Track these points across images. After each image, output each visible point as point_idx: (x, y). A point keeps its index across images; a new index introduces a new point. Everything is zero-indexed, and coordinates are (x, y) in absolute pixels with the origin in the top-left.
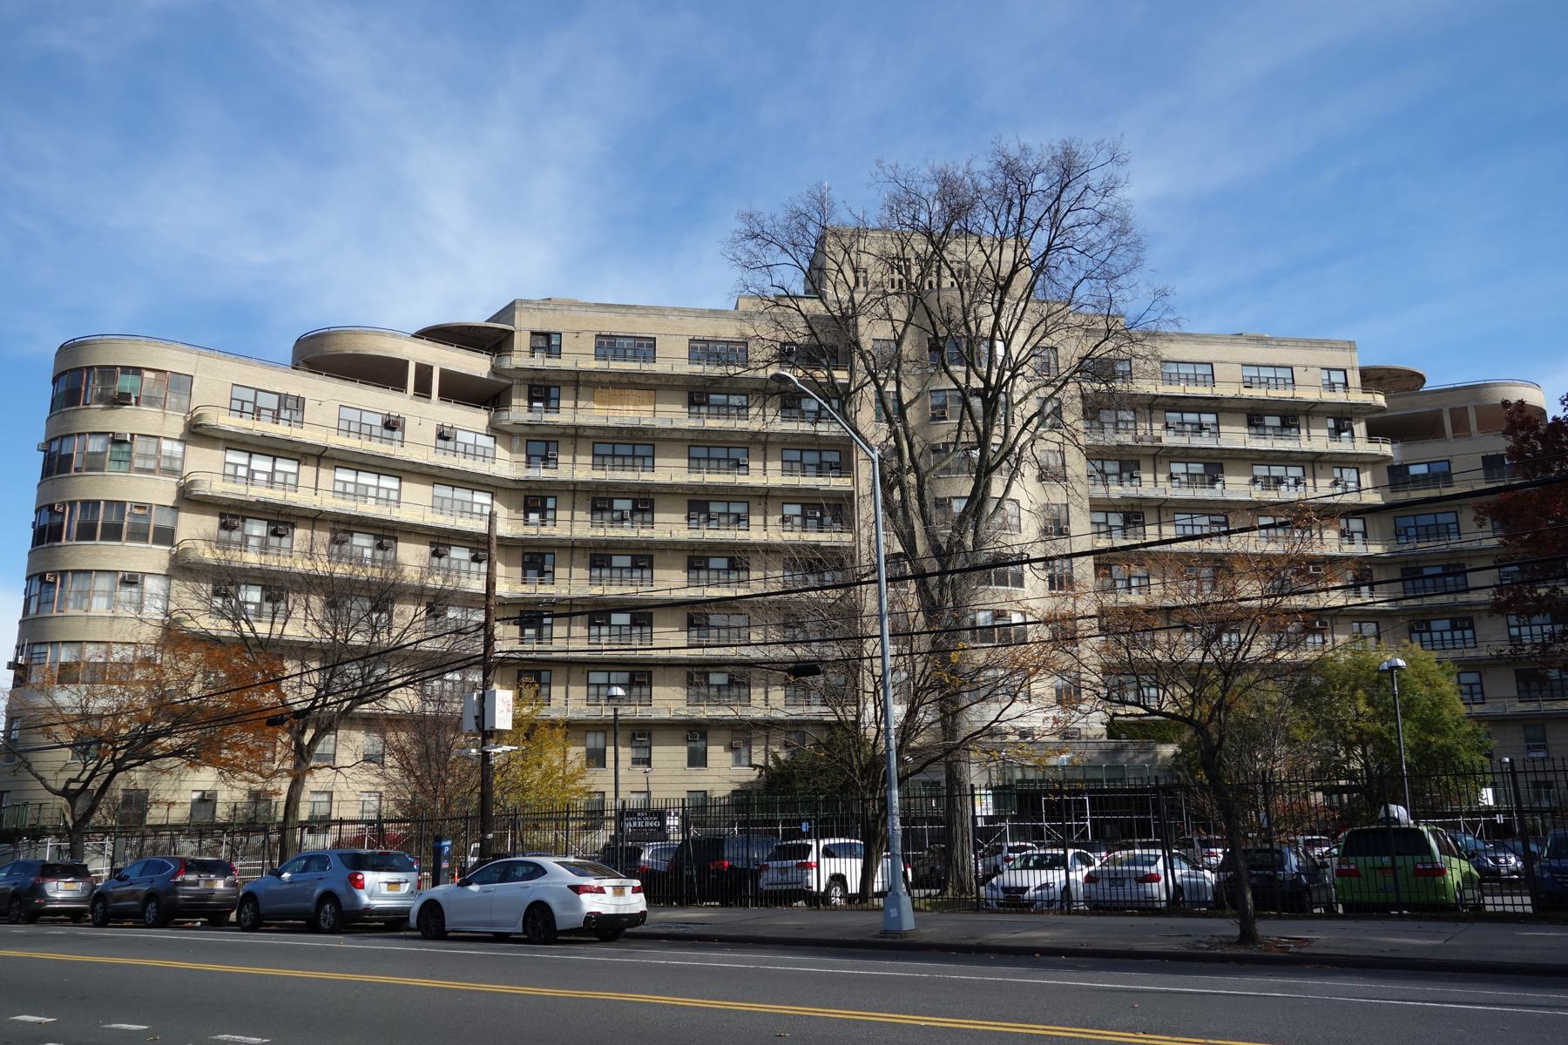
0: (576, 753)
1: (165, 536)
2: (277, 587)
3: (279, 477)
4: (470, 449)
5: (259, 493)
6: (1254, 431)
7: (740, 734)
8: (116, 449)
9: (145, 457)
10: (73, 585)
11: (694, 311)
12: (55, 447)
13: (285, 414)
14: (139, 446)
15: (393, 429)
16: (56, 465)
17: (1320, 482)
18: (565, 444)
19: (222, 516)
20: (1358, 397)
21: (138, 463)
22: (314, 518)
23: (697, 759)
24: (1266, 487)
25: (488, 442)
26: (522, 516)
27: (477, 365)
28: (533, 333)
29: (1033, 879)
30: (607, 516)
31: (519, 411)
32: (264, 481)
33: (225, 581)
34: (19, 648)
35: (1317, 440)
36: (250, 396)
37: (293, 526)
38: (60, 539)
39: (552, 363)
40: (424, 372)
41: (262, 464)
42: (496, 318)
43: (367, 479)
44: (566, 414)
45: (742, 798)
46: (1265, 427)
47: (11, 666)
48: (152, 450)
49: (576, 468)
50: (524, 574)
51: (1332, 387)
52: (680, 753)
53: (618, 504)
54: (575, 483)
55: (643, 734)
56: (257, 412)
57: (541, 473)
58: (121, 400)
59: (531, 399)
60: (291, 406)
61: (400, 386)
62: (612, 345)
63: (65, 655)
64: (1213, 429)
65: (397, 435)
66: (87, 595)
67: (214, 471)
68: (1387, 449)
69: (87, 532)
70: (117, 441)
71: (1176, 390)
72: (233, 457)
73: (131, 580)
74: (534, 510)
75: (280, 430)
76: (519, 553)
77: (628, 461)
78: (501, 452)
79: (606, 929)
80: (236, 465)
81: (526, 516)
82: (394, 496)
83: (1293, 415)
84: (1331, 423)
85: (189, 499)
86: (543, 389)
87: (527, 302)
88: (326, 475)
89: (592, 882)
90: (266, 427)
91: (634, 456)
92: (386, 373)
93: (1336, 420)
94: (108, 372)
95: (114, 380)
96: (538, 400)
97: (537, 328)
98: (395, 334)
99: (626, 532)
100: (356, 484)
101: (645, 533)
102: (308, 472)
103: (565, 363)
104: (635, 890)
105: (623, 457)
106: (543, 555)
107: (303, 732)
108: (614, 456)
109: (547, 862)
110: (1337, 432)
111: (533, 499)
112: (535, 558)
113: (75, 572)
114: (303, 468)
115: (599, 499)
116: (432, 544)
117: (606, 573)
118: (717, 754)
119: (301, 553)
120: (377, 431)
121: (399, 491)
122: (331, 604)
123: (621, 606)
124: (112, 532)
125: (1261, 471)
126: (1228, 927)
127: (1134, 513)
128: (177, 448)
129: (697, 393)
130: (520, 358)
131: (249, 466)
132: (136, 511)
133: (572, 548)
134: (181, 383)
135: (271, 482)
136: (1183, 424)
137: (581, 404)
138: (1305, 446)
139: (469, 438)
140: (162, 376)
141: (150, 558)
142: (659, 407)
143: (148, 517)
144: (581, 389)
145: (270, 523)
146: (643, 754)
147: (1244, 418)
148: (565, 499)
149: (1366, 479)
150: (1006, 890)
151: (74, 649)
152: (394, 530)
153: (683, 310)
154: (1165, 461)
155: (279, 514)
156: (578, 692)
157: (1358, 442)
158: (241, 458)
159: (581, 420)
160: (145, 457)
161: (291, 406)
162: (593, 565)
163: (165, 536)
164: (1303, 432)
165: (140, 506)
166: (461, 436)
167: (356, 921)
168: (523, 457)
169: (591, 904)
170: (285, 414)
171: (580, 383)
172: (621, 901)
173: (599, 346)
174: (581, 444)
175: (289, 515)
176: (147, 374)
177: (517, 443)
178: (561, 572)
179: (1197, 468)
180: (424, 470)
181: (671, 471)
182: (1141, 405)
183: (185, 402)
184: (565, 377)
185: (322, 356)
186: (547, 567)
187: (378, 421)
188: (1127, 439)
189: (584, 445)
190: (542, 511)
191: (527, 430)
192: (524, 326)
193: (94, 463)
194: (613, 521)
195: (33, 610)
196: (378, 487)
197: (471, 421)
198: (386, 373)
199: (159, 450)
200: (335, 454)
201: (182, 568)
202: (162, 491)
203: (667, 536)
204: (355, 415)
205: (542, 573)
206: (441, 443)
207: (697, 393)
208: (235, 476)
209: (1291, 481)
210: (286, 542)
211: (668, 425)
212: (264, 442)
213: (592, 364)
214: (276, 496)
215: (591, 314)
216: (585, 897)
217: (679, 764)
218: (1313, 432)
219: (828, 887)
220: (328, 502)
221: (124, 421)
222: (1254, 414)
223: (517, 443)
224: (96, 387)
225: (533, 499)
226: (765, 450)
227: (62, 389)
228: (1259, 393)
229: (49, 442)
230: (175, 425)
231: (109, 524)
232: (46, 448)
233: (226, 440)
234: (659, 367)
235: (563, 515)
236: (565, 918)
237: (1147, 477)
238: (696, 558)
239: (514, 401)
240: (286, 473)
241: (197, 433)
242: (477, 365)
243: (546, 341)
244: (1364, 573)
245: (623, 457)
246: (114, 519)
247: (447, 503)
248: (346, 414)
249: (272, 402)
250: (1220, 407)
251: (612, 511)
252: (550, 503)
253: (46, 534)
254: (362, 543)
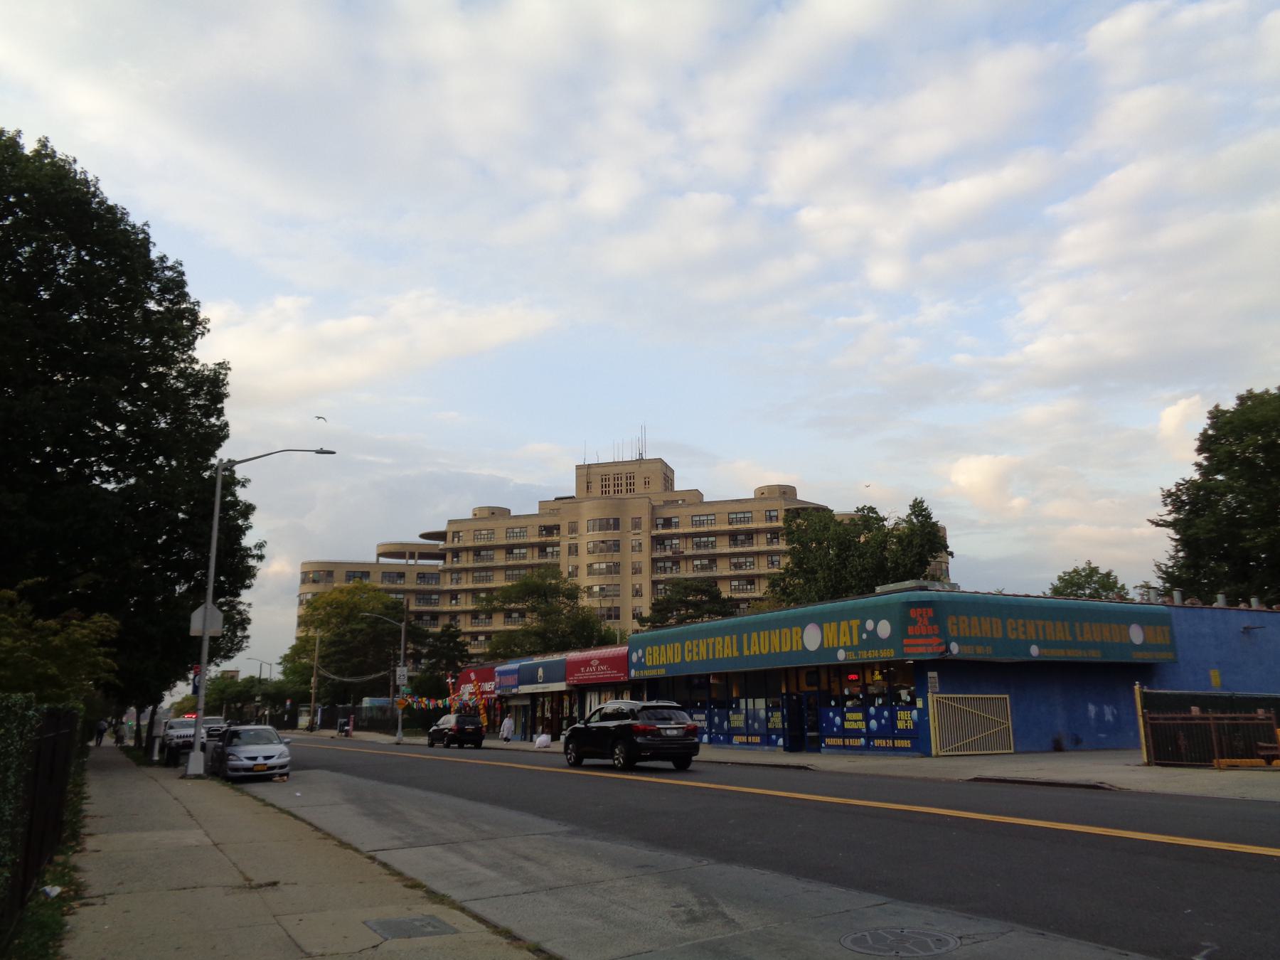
35: (761, 545)
51: (771, 519)
83: (750, 535)
103: (461, 544)
110: (770, 542)
125: (734, 560)
138: (755, 548)
157: (782, 546)
179: (706, 562)
188: (669, 553)
190: (456, 598)
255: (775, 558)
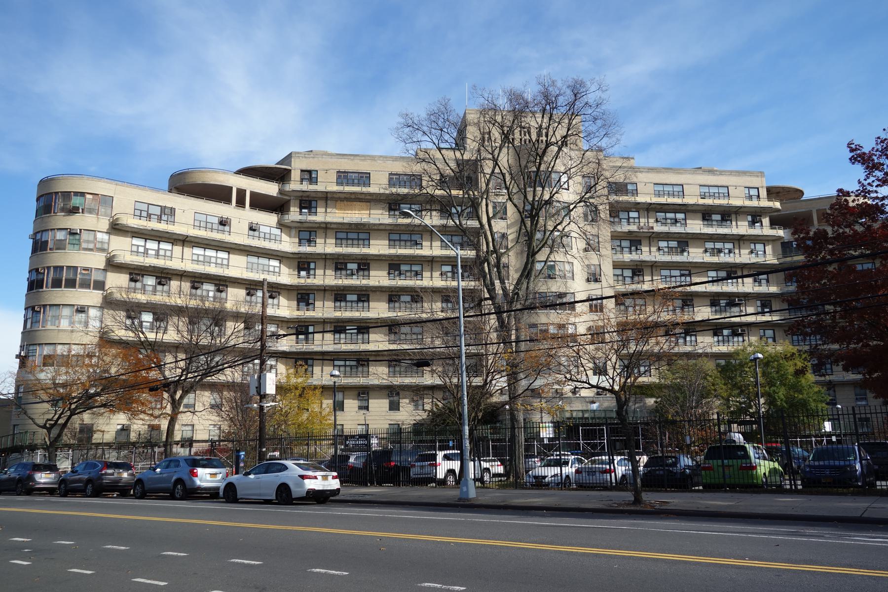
0: (328, 403)
1: (100, 285)
2: (162, 314)
3: (162, 253)
4: (267, 236)
5: (151, 261)
6: (706, 223)
7: (418, 392)
8: (71, 238)
9: (88, 242)
10: (50, 313)
11: (391, 157)
12: (39, 236)
13: (164, 218)
14: (85, 236)
15: (225, 225)
16: (39, 246)
17: (742, 251)
18: (320, 232)
19: (130, 274)
20: (765, 203)
21: (84, 245)
22: (181, 275)
23: (394, 407)
24: (712, 254)
25: (278, 232)
26: (296, 273)
27: (270, 189)
28: (302, 171)
29: (550, 472)
30: (344, 272)
31: (294, 214)
32: (152, 255)
33: (133, 310)
34: (22, 347)
35: (742, 228)
36: (145, 207)
37: (170, 279)
38: (42, 288)
39: (312, 187)
40: (241, 193)
41: (152, 245)
42: (281, 162)
43: (210, 253)
44: (321, 215)
45: (418, 428)
46: (712, 221)
47: (18, 356)
48: (91, 238)
49: (327, 246)
50: (298, 305)
51: (750, 197)
52: (385, 403)
53: (350, 266)
54: (326, 255)
55: (364, 393)
56: (149, 216)
57: (307, 249)
58: (74, 211)
59: (301, 208)
60: (168, 213)
61: (228, 201)
62: (346, 177)
63: (47, 350)
64: (683, 222)
65: (227, 228)
66: (58, 318)
67: (125, 249)
68: (781, 233)
69: (57, 284)
70: (72, 233)
71: (662, 200)
72: (136, 241)
73: (81, 310)
74: (303, 270)
75: (162, 227)
76: (295, 293)
77: (355, 242)
78: (285, 237)
79: (320, 498)
80: (138, 246)
81: (299, 273)
82: (225, 262)
83: (728, 214)
84: (750, 218)
85: (113, 265)
86: (307, 202)
87: (298, 153)
88: (187, 250)
89: (310, 473)
90: (154, 225)
91: (358, 239)
92: (220, 194)
93: (752, 216)
94: (67, 195)
95: (70, 199)
96: (305, 208)
97: (304, 168)
98: (225, 171)
99: (354, 281)
100: (204, 256)
101: (365, 282)
102: (177, 249)
103: (320, 187)
104: (334, 478)
105: (353, 239)
106: (308, 295)
107: (175, 392)
108: (347, 239)
109: (289, 463)
110: (753, 223)
111: (303, 263)
112: (304, 296)
113: (51, 305)
114: (175, 247)
115: (339, 263)
116: (247, 289)
117: (343, 304)
118: (405, 403)
119: (177, 294)
120: (215, 226)
121: (228, 259)
122: (191, 322)
123: (350, 321)
124: (71, 284)
125: (709, 245)
126: (629, 496)
127: (638, 270)
128: (105, 237)
129: (393, 203)
130: (295, 185)
131: (145, 246)
132: (84, 272)
133: (324, 290)
134: (107, 201)
135: (157, 255)
136: (666, 219)
137: (329, 210)
139: (267, 230)
140: (96, 197)
141: (92, 297)
142: (372, 212)
143: (90, 275)
144: (329, 202)
145: (157, 277)
146: (364, 404)
147: (700, 215)
148: (320, 263)
149: (769, 249)
150: (535, 477)
151: (52, 347)
152: (225, 281)
153: (386, 157)
154: (656, 240)
155: (162, 273)
156: (328, 369)
157: (765, 229)
158: (141, 242)
159: (329, 219)
160: (88, 242)
161: (168, 213)
162: (336, 300)
163: (100, 285)
164: (734, 223)
165: (86, 269)
166: (262, 229)
167: (193, 494)
168: (297, 240)
169: (310, 484)
170: (164, 218)
171: (328, 198)
172: (326, 483)
173: (339, 177)
174: (329, 232)
175: (168, 273)
176: (88, 196)
177: (293, 232)
178: (318, 304)
179: (674, 244)
180: (242, 248)
181: (379, 247)
182: (643, 209)
183: (109, 211)
184: (320, 195)
185: (185, 185)
186: (311, 301)
187: (216, 220)
188: (633, 228)
189: (331, 233)
190: (308, 270)
191: (299, 225)
192: (296, 167)
193: (60, 246)
194: (347, 275)
195: (29, 326)
196: (217, 258)
197: (267, 220)
198: (220, 194)
199: (95, 238)
200: (193, 240)
201: (109, 303)
202: (97, 261)
203: (377, 284)
204: (203, 218)
205: (308, 304)
206: (251, 233)
207: (393, 203)
208: (138, 252)
209: (727, 251)
210: (166, 288)
211: (377, 222)
212: (153, 233)
213: (334, 188)
214: (160, 263)
215: (334, 160)
216: (307, 481)
217: (384, 409)
218: (739, 223)
219: (446, 476)
220: (190, 267)
221: (75, 222)
222: (706, 214)
223: (293, 232)
224: (60, 204)
225: (303, 263)
226: (431, 235)
227: (42, 204)
228: (709, 201)
229: (35, 234)
230: (104, 224)
231: (69, 279)
232: (34, 237)
233: (132, 232)
234: (373, 189)
235: (319, 272)
236: (296, 492)
237: (645, 249)
238: (393, 296)
239: (292, 209)
240: (166, 250)
241: (116, 228)
242: (270, 189)
243: (309, 175)
244: (765, 302)
245: (353, 239)
246: (71, 276)
247: (255, 266)
248: (198, 217)
249: (157, 211)
250: (687, 210)
251: (346, 269)
252: (312, 266)
253: (35, 285)
254: (209, 289)
255: (759, 247)
